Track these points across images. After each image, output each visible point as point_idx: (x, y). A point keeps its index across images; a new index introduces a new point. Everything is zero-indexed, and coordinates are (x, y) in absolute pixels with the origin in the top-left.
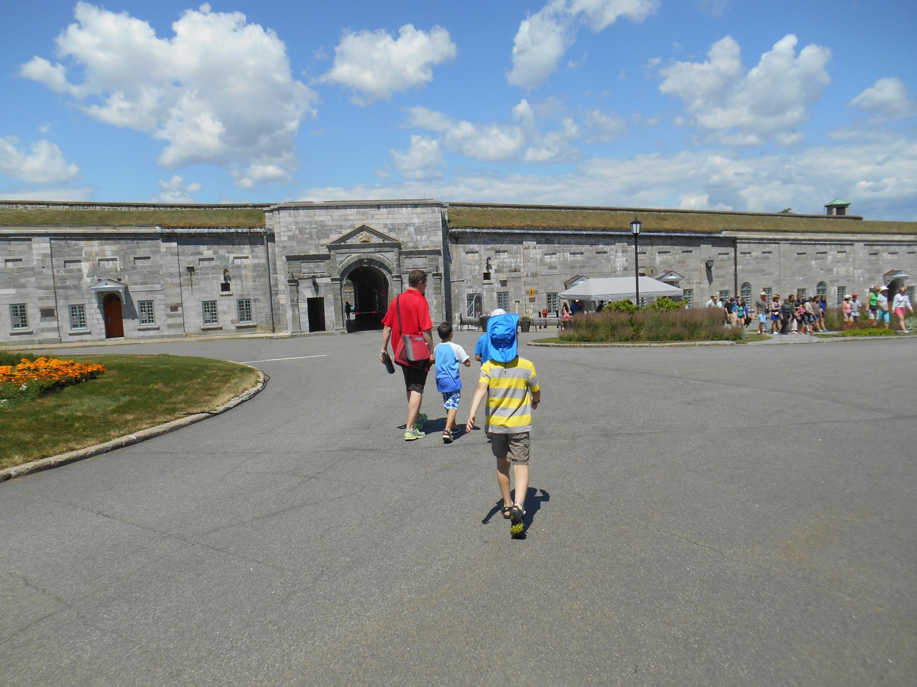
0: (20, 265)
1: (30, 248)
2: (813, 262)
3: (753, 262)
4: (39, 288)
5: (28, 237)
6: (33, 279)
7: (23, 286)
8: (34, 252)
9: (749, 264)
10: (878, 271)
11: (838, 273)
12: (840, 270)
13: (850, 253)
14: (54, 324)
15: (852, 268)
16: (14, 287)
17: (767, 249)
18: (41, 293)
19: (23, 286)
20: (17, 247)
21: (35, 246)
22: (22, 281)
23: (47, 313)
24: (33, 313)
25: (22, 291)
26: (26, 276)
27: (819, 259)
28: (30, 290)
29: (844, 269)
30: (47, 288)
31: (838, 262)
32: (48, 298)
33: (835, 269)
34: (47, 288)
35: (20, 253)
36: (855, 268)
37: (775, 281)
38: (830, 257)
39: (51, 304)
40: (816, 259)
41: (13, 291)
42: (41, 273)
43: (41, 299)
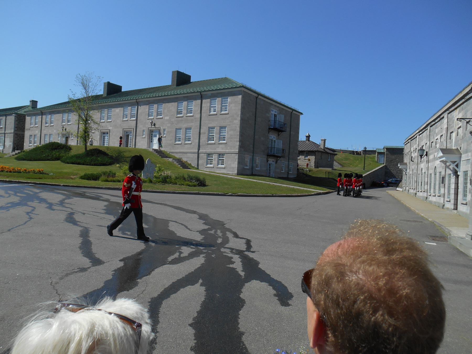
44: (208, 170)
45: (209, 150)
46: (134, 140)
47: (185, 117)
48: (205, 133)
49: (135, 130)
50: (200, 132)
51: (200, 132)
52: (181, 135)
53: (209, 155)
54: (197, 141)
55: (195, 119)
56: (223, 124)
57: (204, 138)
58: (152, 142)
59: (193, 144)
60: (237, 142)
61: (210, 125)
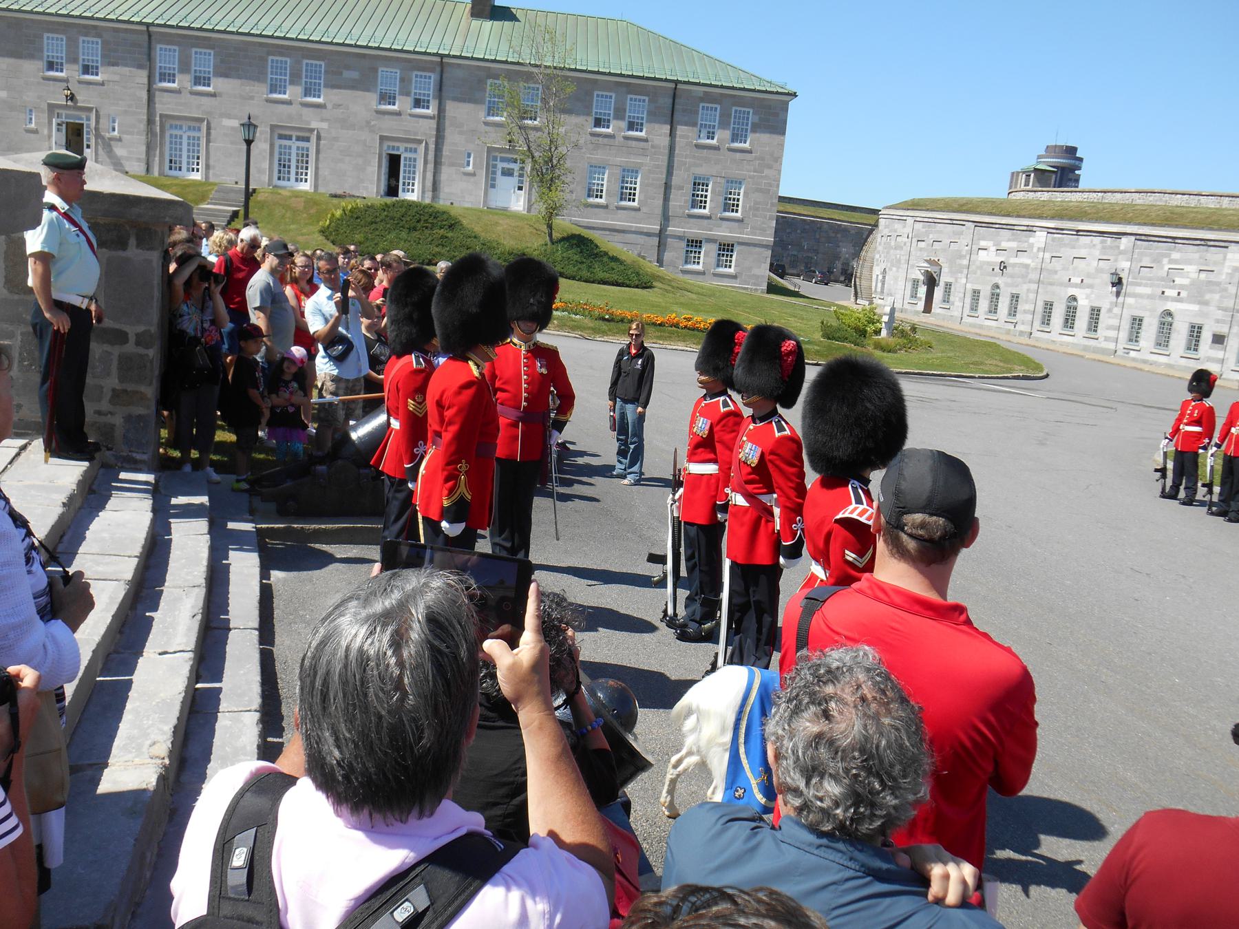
0: (1212, 277)
1: (1225, 258)
4: (1220, 308)
5: (1223, 245)
6: (1217, 296)
7: (1206, 303)
8: (1227, 263)
14: (1220, 354)
16: (1200, 303)
18: (1220, 314)
19: (1206, 303)
20: (1213, 254)
21: (1229, 256)
22: (1208, 297)
23: (1219, 339)
24: (1206, 337)
25: (1205, 308)
26: (1212, 292)
28: (1212, 308)
30: (1225, 310)
32: (1223, 322)
34: (1225, 310)
35: (1215, 263)
39: (1223, 329)
41: (1195, 307)
42: (1225, 290)
43: (1218, 321)
44: (687, 278)
45: (694, 231)
46: (430, 176)
47: (619, 139)
48: (681, 188)
49: (432, 147)
50: (667, 187)
51: (667, 187)
52: (606, 181)
53: (695, 244)
54: (661, 202)
55: (653, 147)
56: (735, 172)
57: (679, 200)
58: (493, 186)
59: (644, 209)
60: (771, 218)
61: (701, 171)
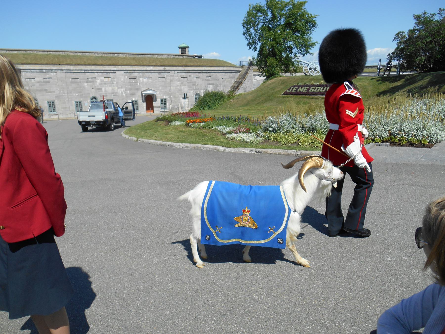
2: (86, 84)
3: (38, 84)
9: (34, 85)
10: (137, 89)
11: (105, 91)
12: (107, 89)
13: (114, 78)
15: (116, 88)
17: (47, 76)
27: (90, 82)
29: (110, 88)
31: (105, 84)
33: (103, 89)
36: (118, 88)
37: (56, 97)
38: (98, 81)
40: (87, 82)
